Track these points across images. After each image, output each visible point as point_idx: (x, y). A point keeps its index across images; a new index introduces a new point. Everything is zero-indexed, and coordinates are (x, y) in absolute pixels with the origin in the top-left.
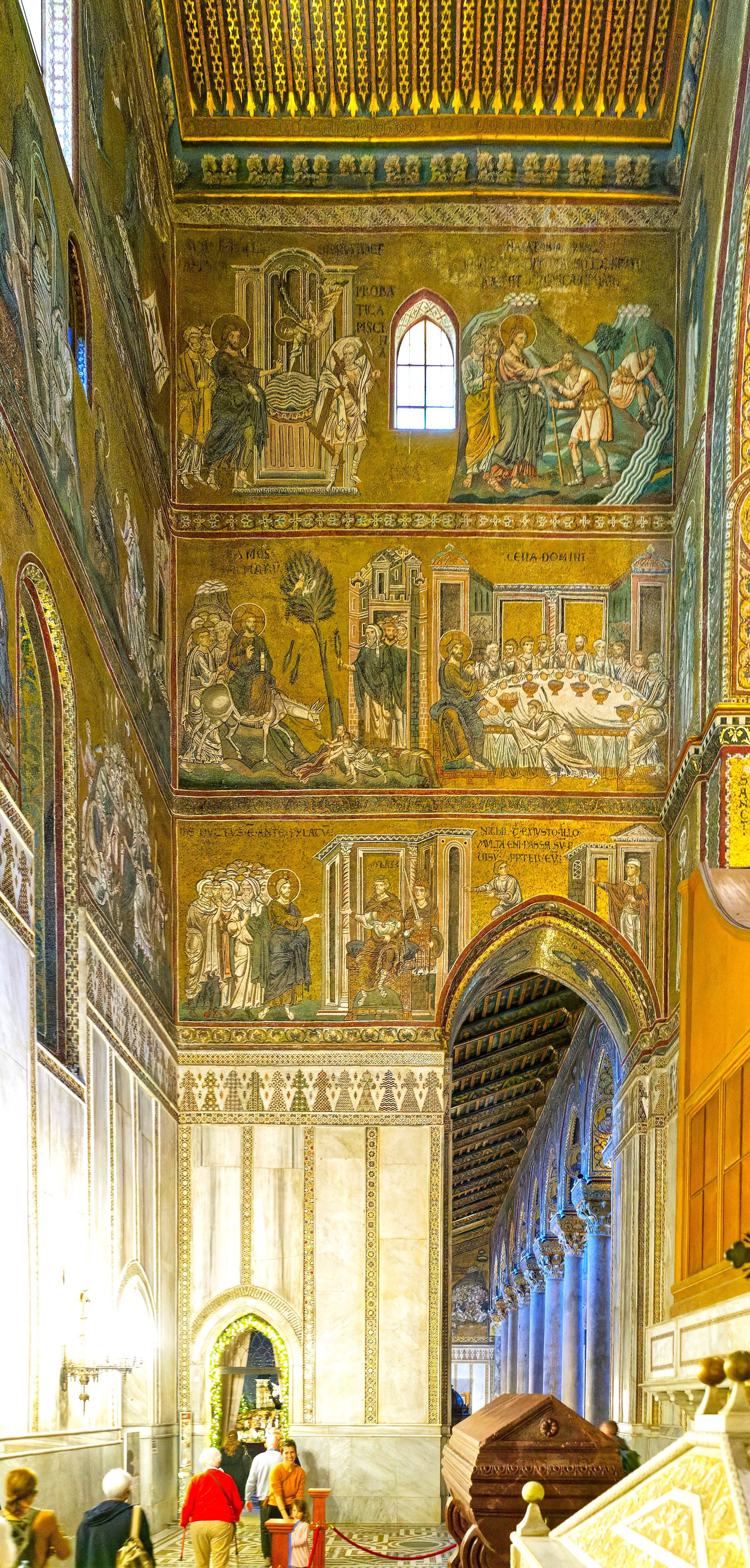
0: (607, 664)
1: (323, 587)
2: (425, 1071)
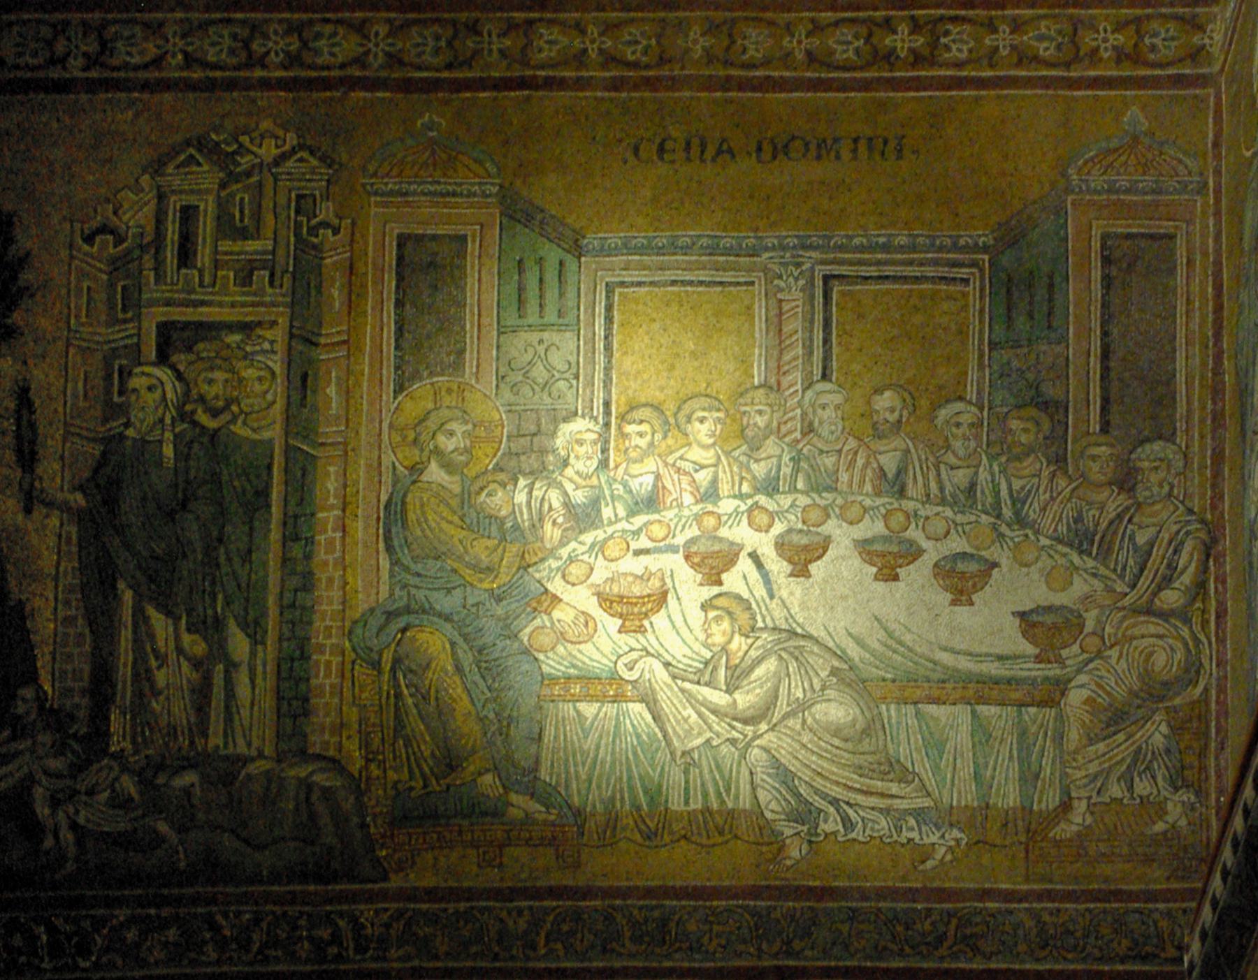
0: (983, 475)
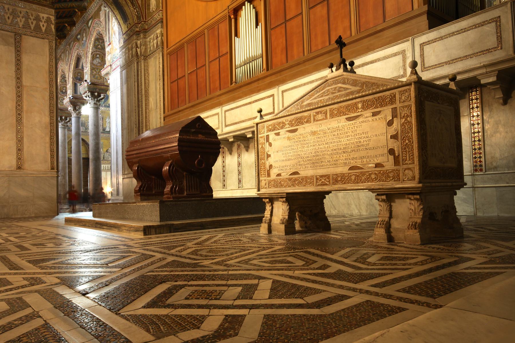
2: (45, 16)
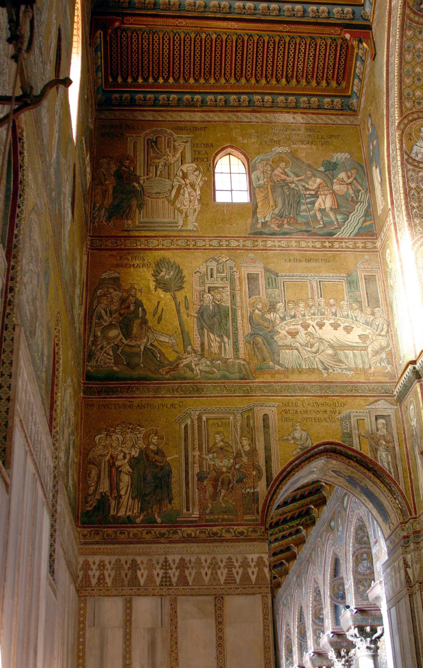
0: (349, 313)
1: (177, 275)
2: (255, 556)
